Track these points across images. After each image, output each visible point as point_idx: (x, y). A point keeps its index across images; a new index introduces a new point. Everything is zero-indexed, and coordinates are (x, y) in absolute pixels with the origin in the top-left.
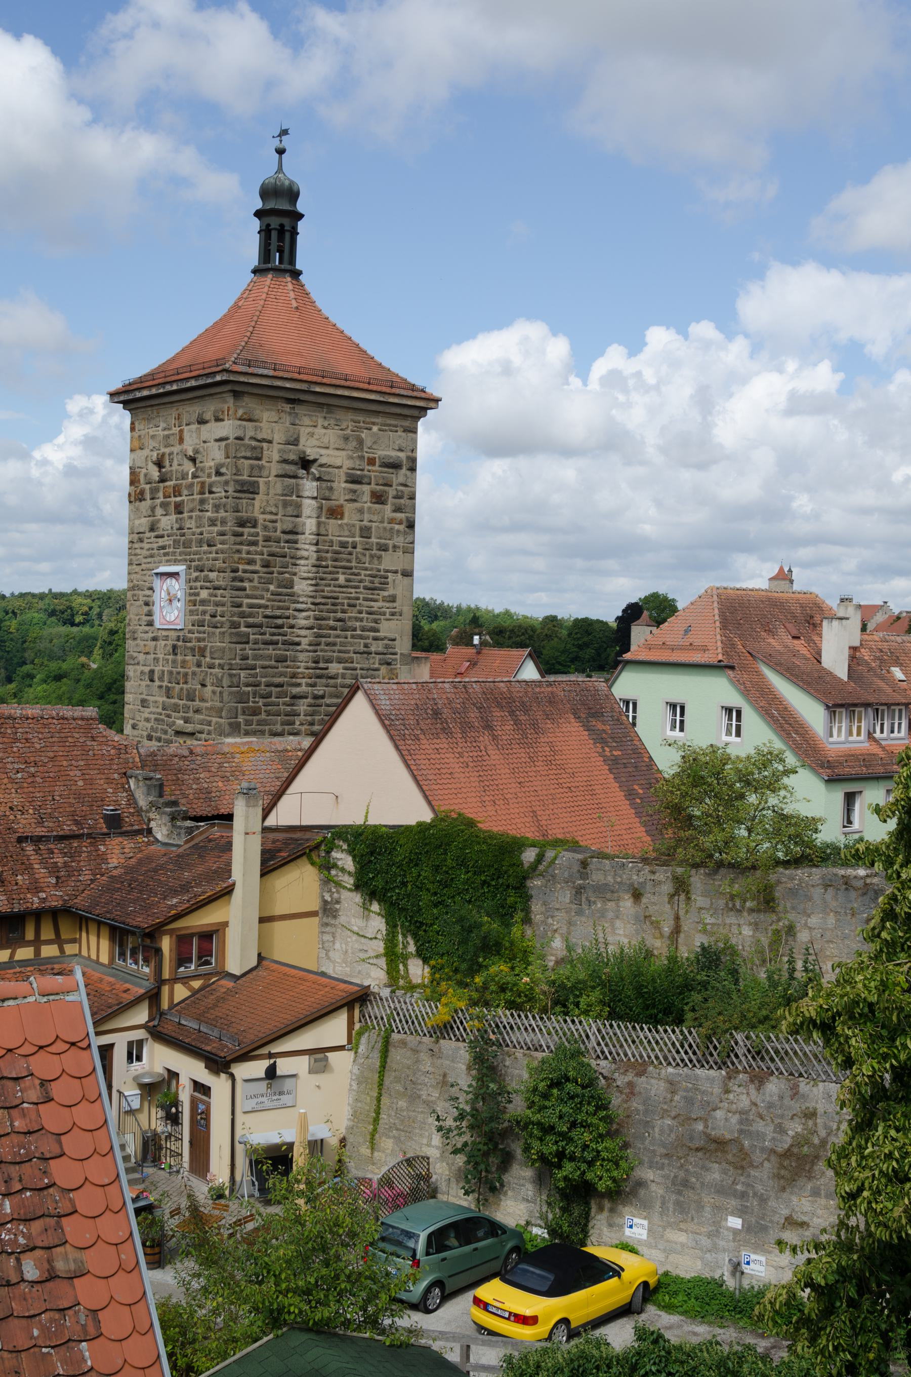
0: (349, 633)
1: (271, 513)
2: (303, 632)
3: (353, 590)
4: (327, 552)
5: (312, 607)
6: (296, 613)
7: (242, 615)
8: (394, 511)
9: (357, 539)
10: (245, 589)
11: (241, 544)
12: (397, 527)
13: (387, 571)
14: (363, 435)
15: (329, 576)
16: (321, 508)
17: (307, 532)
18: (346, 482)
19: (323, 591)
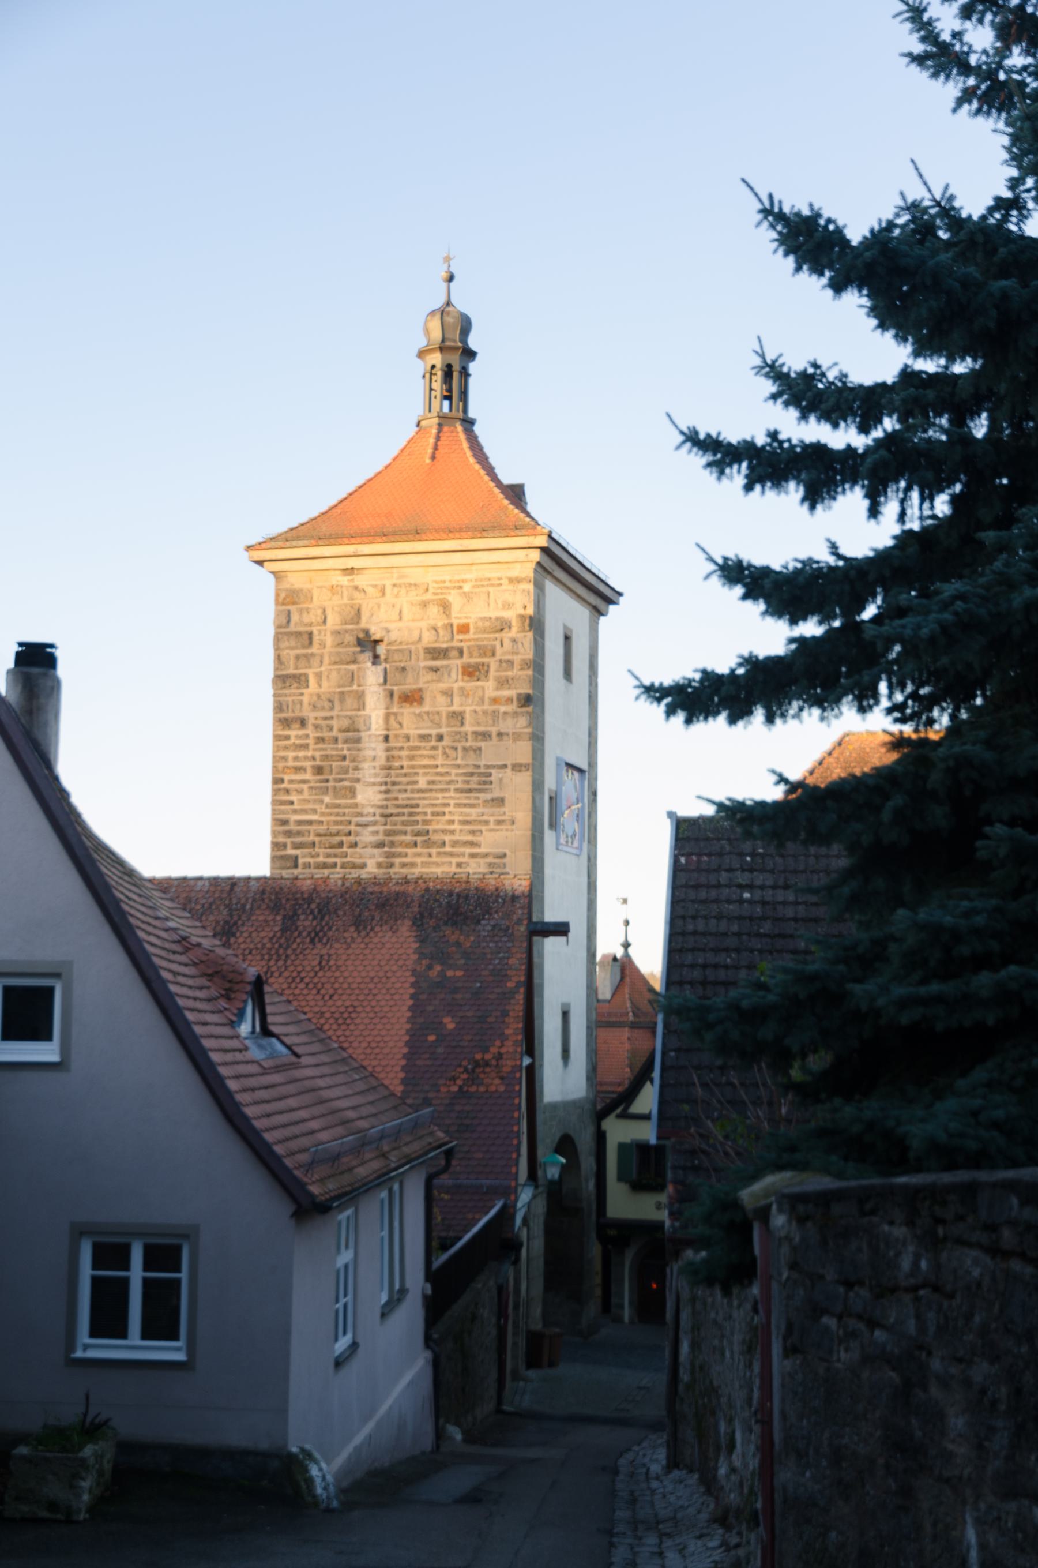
0: (434, 851)
1: (323, 708)
2: (370, 851)
3: (440, 795)
4: (402, 748)
5: (383, 820)
6: (359, 829)
7: (289, 834)
8: (497, 689)
9: (444, 730)
10: (292, 803)
11: (286, 748)
12: (503, 709)
13: (488, 767)
14: (450, 598)
15: (404, 780)
16: (391, 694)
17: (374, 726)
18: (425, 659)
19: (396, 799)
